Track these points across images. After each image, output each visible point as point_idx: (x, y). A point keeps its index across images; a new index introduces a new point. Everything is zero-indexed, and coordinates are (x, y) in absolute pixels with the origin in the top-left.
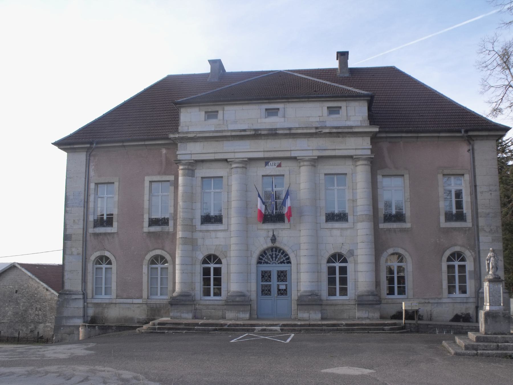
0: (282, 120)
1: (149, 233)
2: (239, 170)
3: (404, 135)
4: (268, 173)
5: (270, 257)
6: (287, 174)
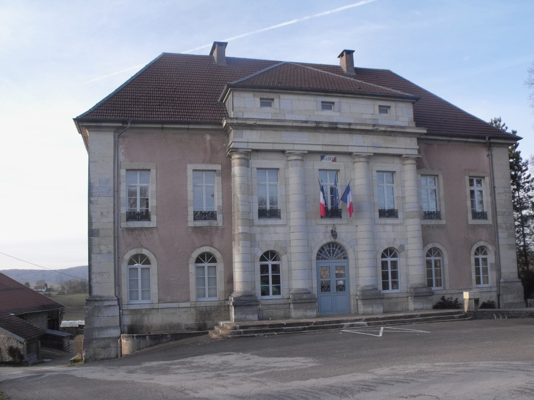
0: (338, 114)
1: (195, 228)
2: (299, 162)
3: (440, 138)
4: (324, 167)
5: (327, 252)
6: (342, 168)
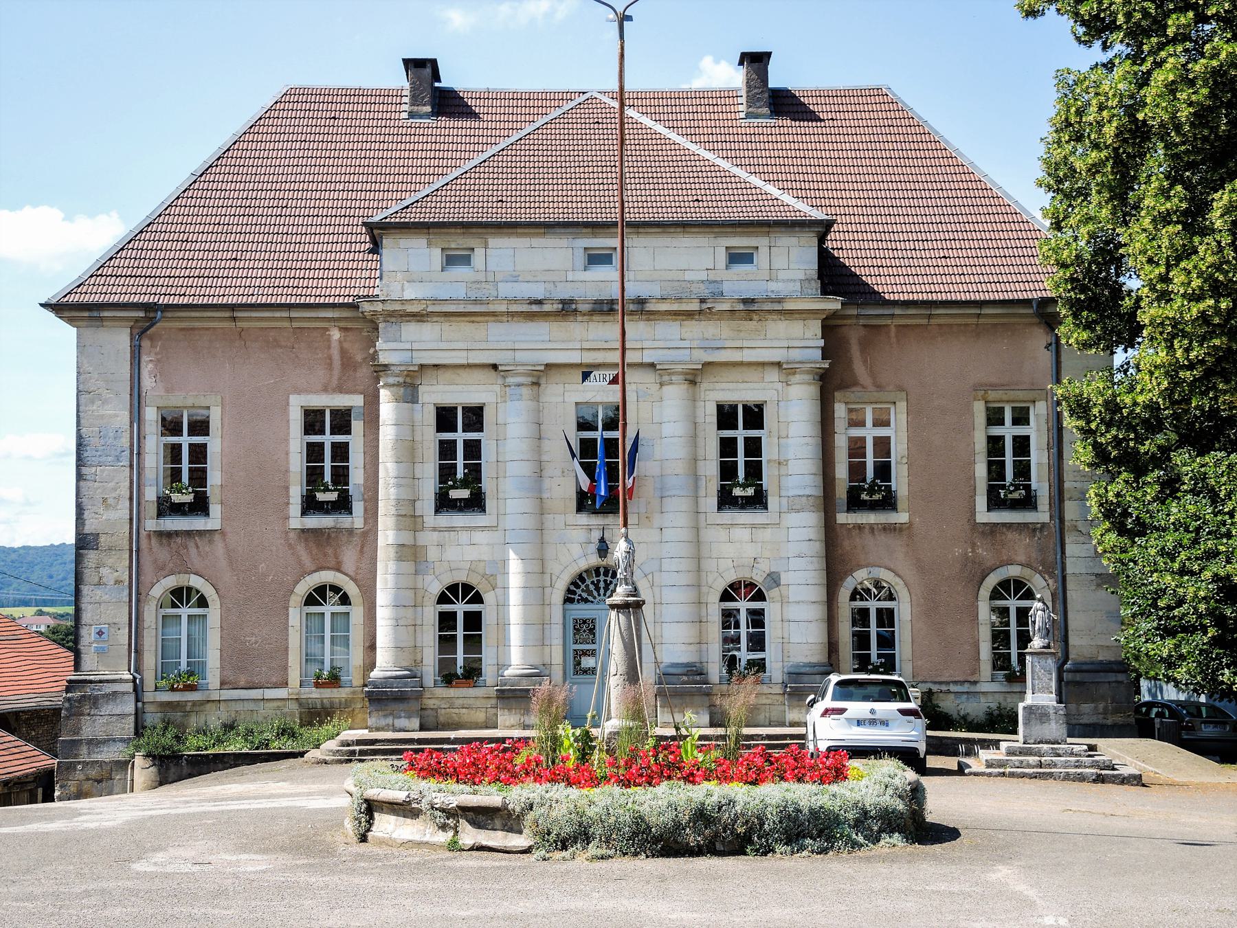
5: (592, 587)
